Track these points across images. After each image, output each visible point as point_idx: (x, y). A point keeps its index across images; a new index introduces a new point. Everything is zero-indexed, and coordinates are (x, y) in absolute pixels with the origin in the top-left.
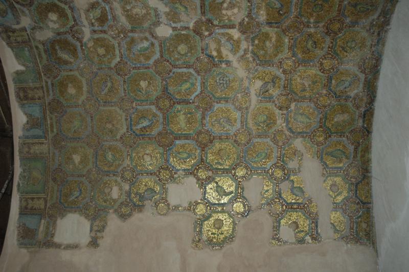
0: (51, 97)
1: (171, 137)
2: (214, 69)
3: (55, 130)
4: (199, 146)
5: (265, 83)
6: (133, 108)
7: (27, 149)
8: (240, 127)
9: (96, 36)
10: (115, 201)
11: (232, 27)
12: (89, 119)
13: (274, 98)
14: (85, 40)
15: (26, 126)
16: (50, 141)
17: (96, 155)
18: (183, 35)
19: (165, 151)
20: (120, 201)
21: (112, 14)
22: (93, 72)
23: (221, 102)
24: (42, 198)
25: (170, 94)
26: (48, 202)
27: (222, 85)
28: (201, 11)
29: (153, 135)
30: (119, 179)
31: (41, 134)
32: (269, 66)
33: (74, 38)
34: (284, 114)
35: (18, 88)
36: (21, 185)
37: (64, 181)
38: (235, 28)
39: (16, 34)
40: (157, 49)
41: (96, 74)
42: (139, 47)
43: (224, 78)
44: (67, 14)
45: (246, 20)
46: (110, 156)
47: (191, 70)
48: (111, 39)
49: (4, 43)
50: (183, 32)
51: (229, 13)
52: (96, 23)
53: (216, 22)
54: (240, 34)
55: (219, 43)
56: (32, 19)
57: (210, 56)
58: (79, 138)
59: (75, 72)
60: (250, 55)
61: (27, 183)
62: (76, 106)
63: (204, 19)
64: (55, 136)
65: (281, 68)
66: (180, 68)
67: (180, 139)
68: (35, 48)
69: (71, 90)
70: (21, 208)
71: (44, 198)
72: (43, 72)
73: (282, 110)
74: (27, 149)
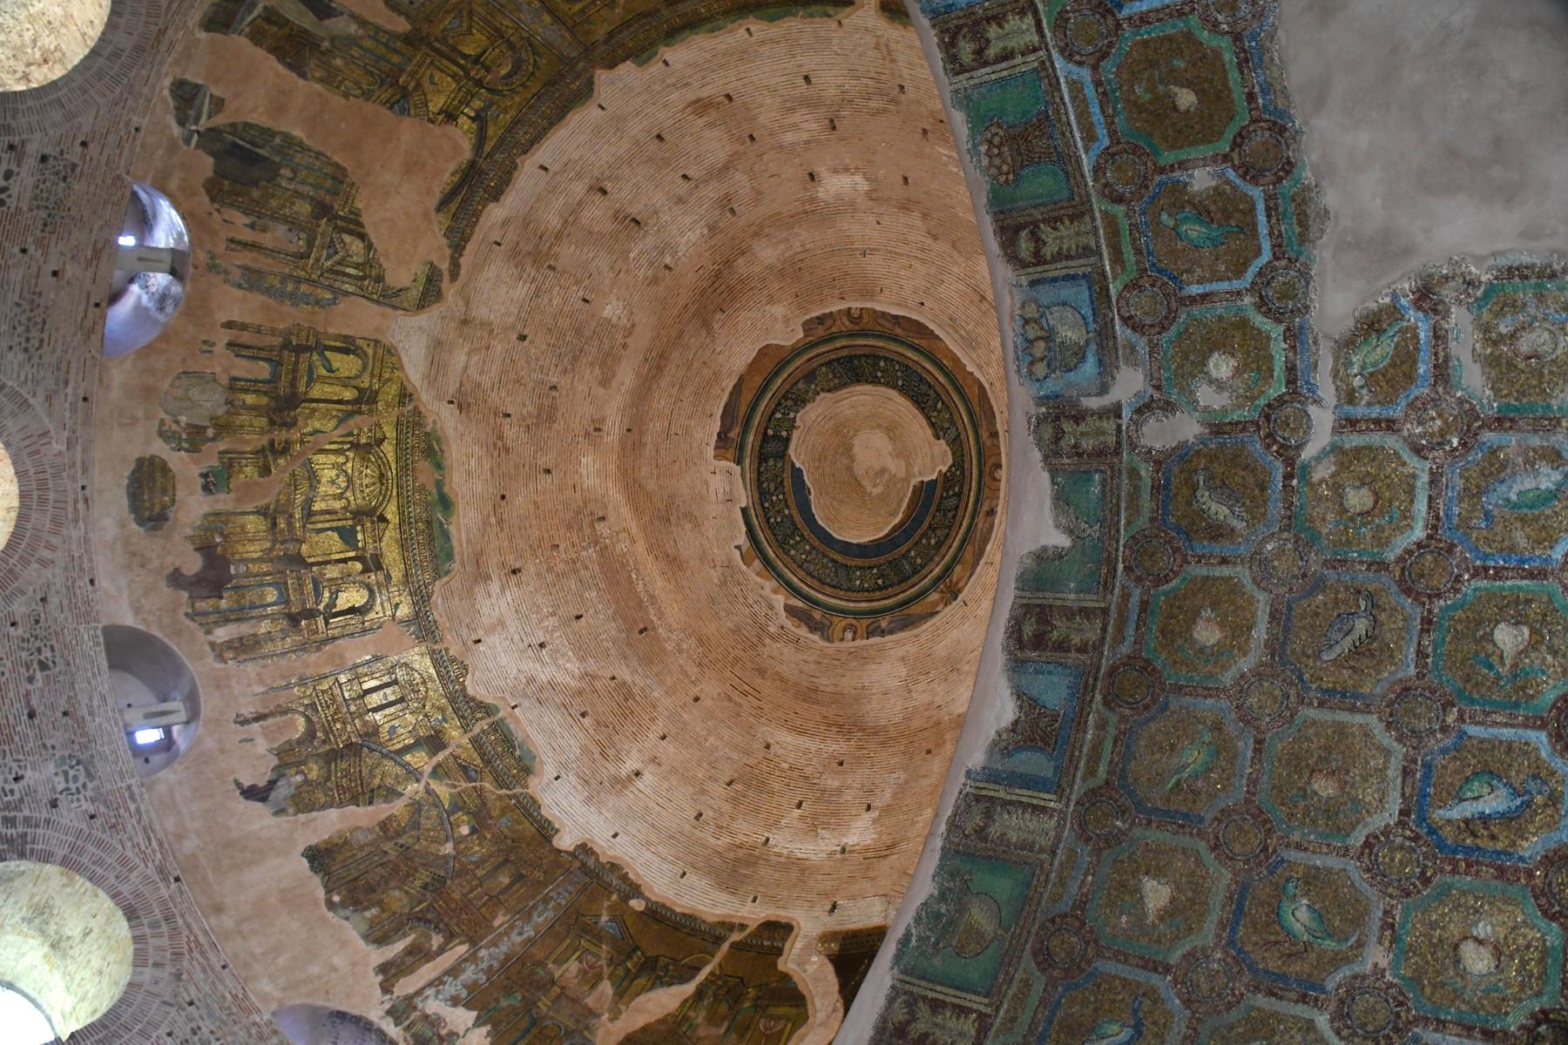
0: (1125, 649)
3: (1102, 771)
6: (1445, 729)
7: (978, 820)
9: (1354, 440)
12: (1246, 748)
14: (1307, 454)
17: (1239, 899)
21: (1436, 354)
22: (1304, 576)
24: (971, 1011)
26: (991, 1033)
29: (1521, 859)
30: (1322, 1021)
33: (1268, 447)
36: (914, 942)
37: (1081, 971)
39: (1083, 427)
41: (1319, 585)
42: (1516, 489)
44: (1271, 357)
46: (1303, 914)
48: (1406, 455)
49: (1037, 455)
52: (1364, 391)
56: (1150, 376)
58: (1186, 816)
59: (1239, 568)
62: (1210, 692)
64: (1093, 793)
68: (1124, 476)
69: (1207, 633)
71: (981, 1015)
72: (1124, 562)
74: (978, 820)
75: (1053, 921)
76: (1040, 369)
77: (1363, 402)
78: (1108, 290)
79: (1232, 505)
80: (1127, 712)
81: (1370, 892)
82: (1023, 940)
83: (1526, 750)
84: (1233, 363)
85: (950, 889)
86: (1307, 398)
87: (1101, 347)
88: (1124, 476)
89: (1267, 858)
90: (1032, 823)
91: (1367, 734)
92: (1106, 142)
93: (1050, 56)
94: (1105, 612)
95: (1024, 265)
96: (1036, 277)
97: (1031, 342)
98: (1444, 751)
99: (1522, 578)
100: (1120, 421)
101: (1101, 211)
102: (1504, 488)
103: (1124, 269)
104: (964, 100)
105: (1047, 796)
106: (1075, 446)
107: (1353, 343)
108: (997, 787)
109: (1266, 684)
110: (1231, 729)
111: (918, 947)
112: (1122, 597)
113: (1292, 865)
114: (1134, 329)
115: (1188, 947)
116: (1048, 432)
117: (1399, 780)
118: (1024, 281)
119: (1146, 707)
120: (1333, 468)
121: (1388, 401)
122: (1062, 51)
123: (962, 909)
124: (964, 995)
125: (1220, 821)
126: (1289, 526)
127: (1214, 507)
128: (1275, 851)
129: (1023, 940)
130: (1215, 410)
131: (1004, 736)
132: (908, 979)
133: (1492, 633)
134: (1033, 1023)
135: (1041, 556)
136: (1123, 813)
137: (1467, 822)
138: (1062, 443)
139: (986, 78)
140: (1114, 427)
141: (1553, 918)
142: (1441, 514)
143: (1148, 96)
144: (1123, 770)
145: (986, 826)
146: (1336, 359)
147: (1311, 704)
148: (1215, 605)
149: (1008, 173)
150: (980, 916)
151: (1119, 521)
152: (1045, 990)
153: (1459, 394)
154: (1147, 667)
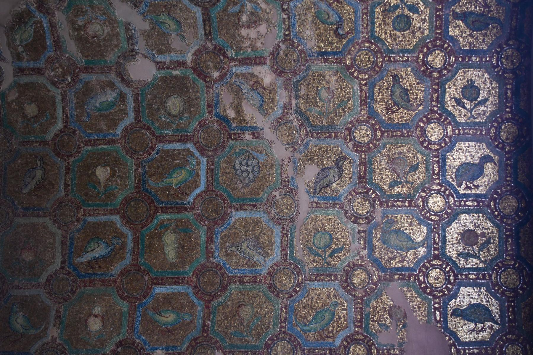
1: (146, 278)
2: (231, 143)
4: (200, 298)
5: (323, 170)
6: (78, 220)
8: (279, 258)
9: (25, 80)
11: (259, 61)
13: (342, 199)
18: (176, 77)
19: (131, 309)
22: (11, 151)
23: (246, 207)
25: (150, 192)
27: (245, 174)
28: (205, 30)
29: (112, 275)
32: (330, 137)
34: (364, 232)
38: (265, 63)
40: (131, 105)
42: (98, 101)
43: (248, 160)
45: (283, 47)
46: (21, 320)
47: (190, 146)
48: (49, 87)
50: (175, 73)
51: (252, 33)
53: (231, 53)
54: (274, 75)
55: (238, 92)
57: (224, 119)
60: (293, 116)
63: (210, 45)
65: (351, 140)
66: (170, 142)
67: (162, 284)
73: (359, 224)
77: (25, 60)
81: (49, 302)
83: (112, 224)
89: (4, 296)
91: (45, 228)
98: (78, 230)
99: (106, 144)
102: (93, 101)
107: (13, 29)
117: (60, 247)
120: (17, 94)
121: (36, 60)
128: (7, 291)
133: (95, 173)
137: (89, 262)
141: (124, 300)
142: (69, 115)
146: (8, 38)
147: (19, 216)
153: (67, 55)
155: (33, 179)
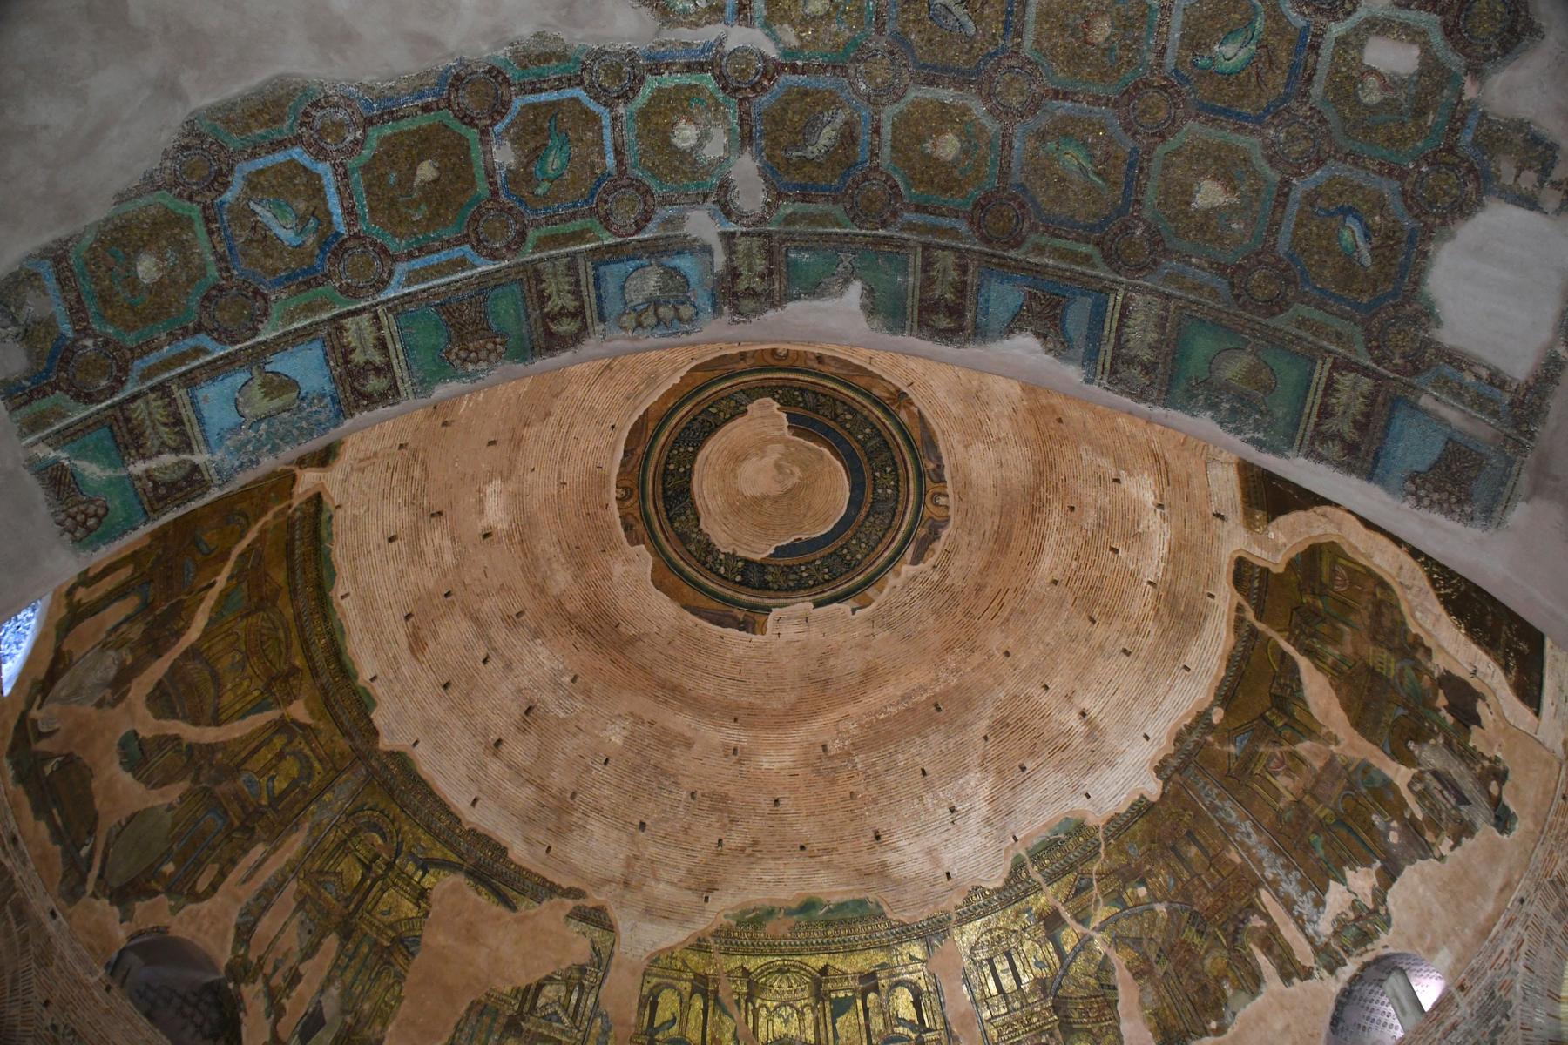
0: (963, 227)
3: (1084, 249)
7: (1136, 371)
10: (1430, 66)
12: (1064, 107)
14: (771, 51)
15: (1051, 346)
16: (1119, 278)
17: (1212, 112)
20: (1437, 39)
22: (891, 53)
24: (1330, 377)
26: (1353, 357)
30: (1337, 29)
31: (1090, 300)
33: (764, 89)
35: (919, 326)
36: (1259, 435)
37: (1288, 268)
41: (900, 38)
44: (678, 88)
46: (1229, 50)
49: (771, 314)
56: (694, 204)
58: (1131, 166)
59: (884, 116)
61: (1262, 413)
64: (1107, 257)
68: (792, 229)
69: (948, 146)
70: (1349, 469)
71: (1334, 367)
74: (1136, 371)
75: (1238, 297)
76: (686, 311)
78: (609, 246)
79: (822, 122)
80: (1026, 225)
82: (1257, 327)
84: (682, 124)
85: (1206, 400)
86: (718, 52)
87: (665, 252)
88: (792, 229)
89: (1173, 86)
90: (1137, 319)
92: (467, 247)
93: (383, 303)
94: (926, 247)
95: (584, 327)
96: (595, 315)
97: (659, 321)
100: (738, 234)
101: (533, 253)
103: (589, 231)
104: (423, 385)
105: (1111, 303)
106: (762, 276)
107: (665, 9)
108: (1102, 353)
109: (999, 89)
110: (1042, 122)
111: (1265, 431)
112: (911, 230)
113: (1180, 61)
114: (648, 220)
115: (1263, 163)
116: (748, 304)
118: (600, 327)
119: (1022, 206)
120: (786, 26)
122: (378, 291)
123: (1226, 387)
124: (1314, 385)
125: (1136, 133)
126: (842, 68)
127: (823, 141)
128: (1165, 78)
129: (1257, 327)
130: (728, 141)
131: (1051, 346)
132: (1298, 442)
134: (1343, 316)
135: (871, 310)
136: (1128, 227)
138: (759, 290)
139: (403, 365)
140: (744, 239)
143: (423, 207)
144: (1084, 228)
145: (1142, 364)
146: (680, 24)
147: (1018, 45)
148: (920, 140)
149: (495, 343)
150: (1233, 369)
151: (836, 234)
152: (1308, 304)
154: (981, 205)
155: (950, 11)
